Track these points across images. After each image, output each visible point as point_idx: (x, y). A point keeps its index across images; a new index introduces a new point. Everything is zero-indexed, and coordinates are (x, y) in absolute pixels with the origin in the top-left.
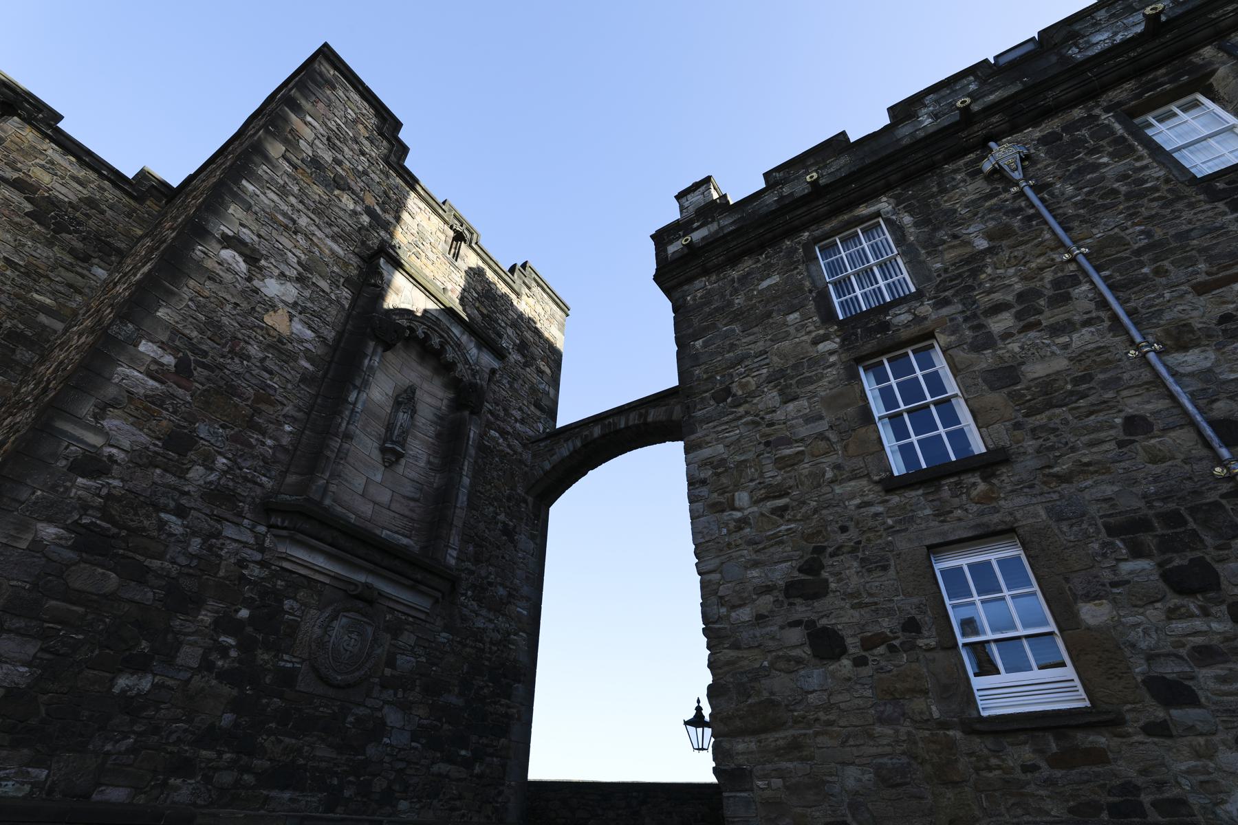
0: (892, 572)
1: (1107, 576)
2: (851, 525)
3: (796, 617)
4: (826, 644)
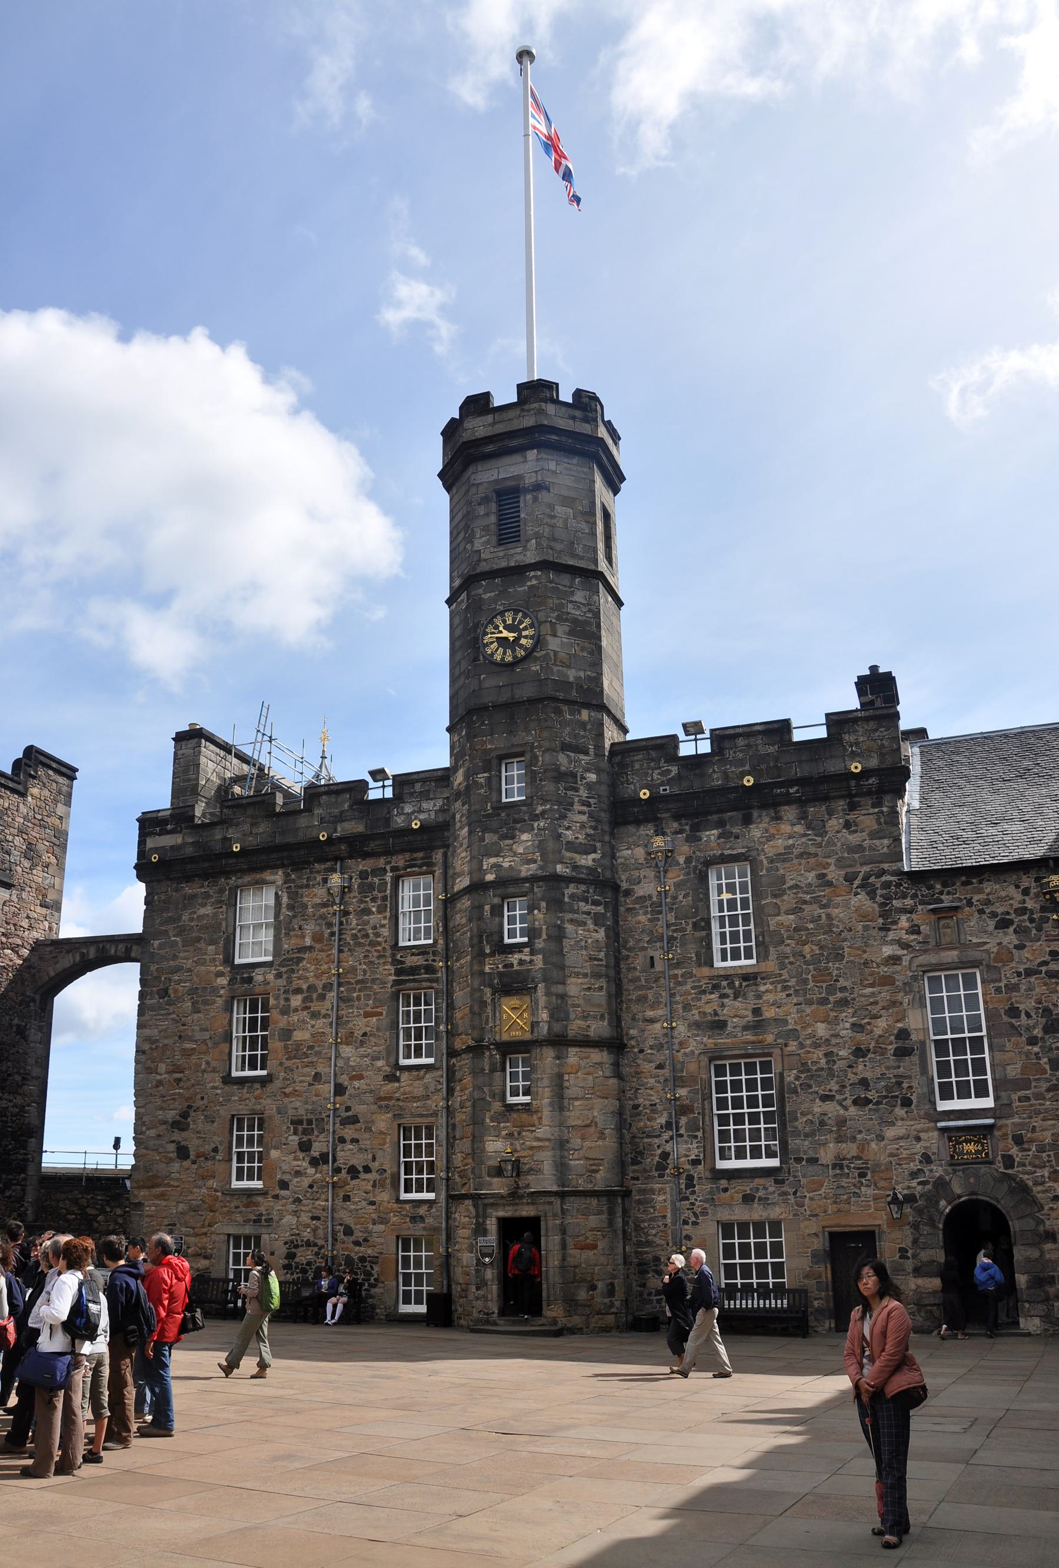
0: (215, 1124)
1: (284, 1140)
2: (206, 1097)
3: (173, 1138)
4: (183, 1153)
